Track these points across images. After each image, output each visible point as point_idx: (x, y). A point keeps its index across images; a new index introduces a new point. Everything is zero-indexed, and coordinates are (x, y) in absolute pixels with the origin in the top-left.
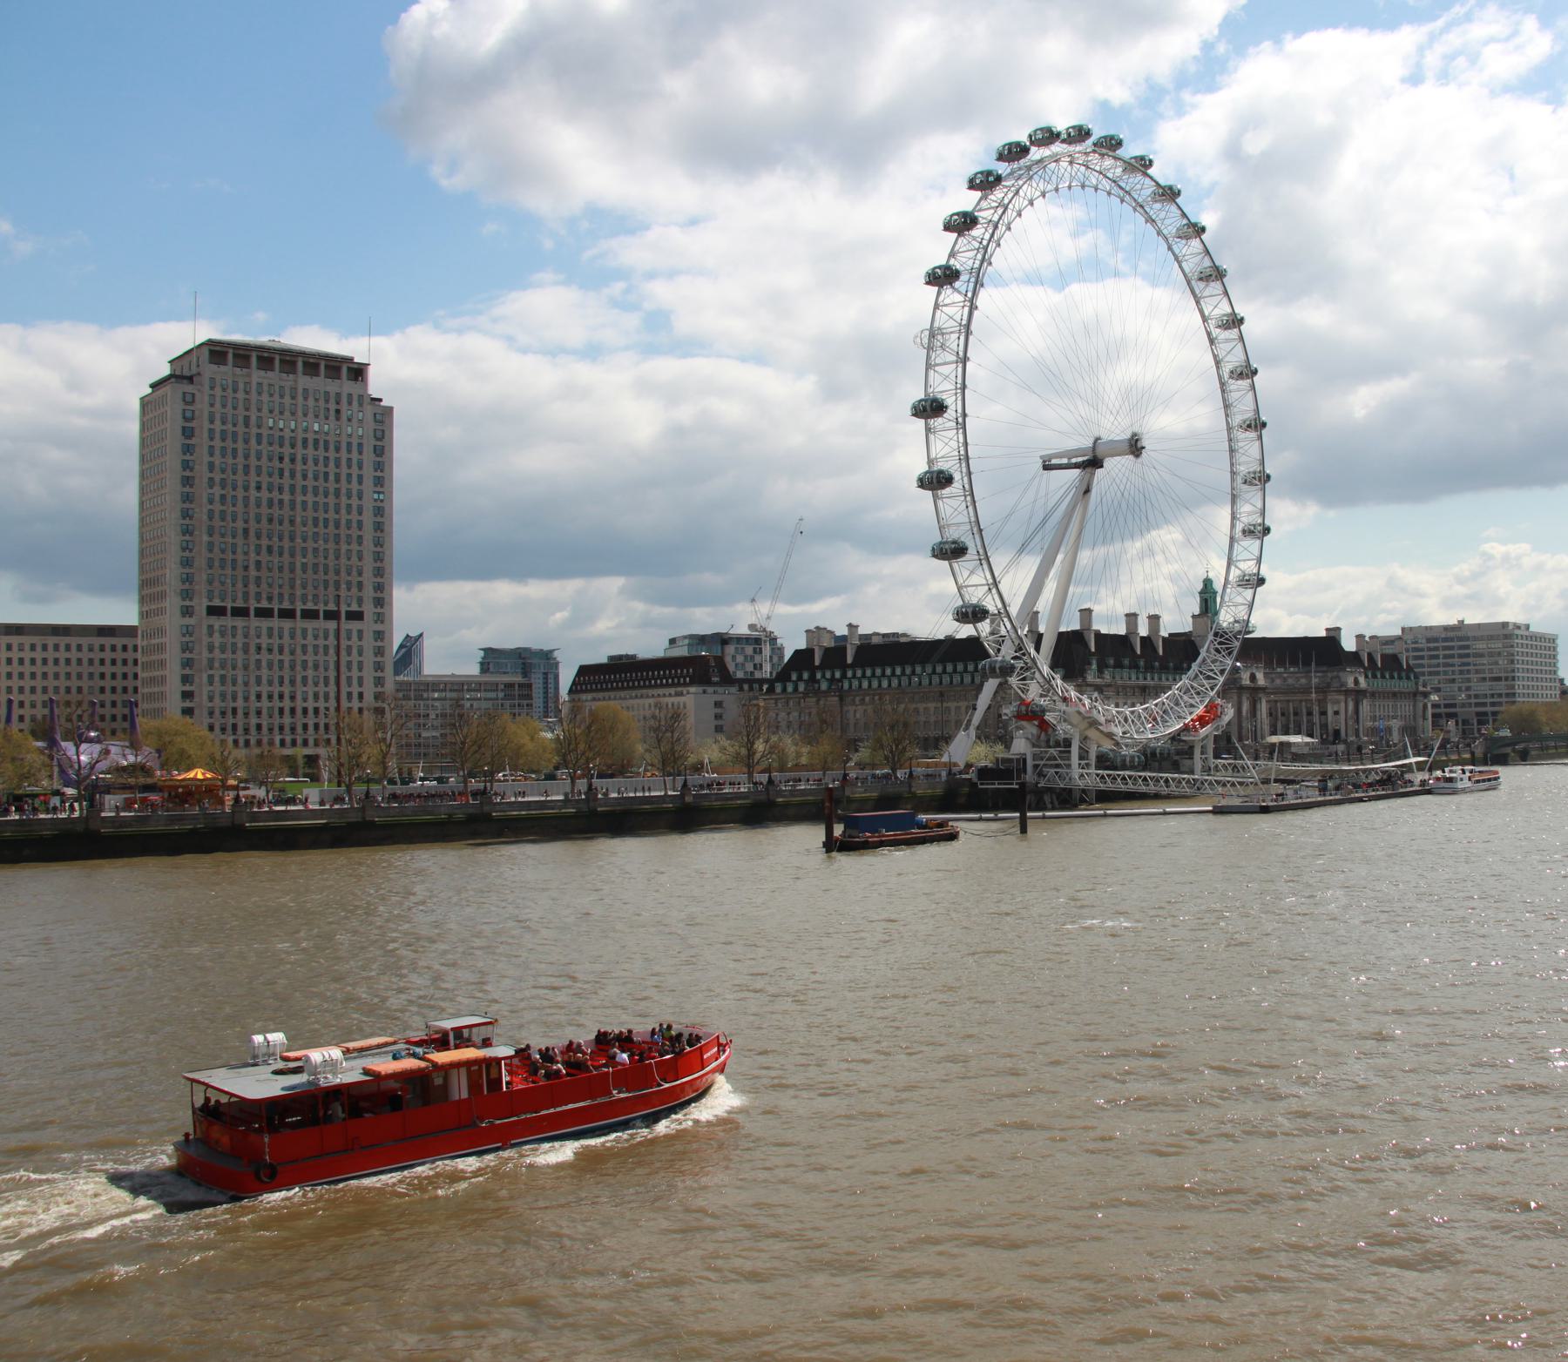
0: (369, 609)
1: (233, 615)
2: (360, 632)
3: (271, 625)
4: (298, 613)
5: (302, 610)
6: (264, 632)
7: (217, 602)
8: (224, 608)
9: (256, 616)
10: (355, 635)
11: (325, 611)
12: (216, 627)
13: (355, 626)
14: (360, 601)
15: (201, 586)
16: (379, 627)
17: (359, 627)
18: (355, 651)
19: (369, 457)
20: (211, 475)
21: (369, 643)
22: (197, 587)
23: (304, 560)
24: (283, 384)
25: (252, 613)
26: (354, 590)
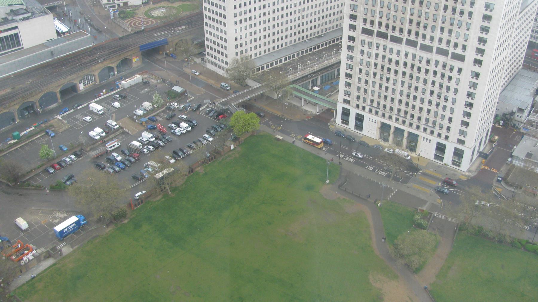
0: (470, 55)
1: (377, 36)
2: (460, 70)
3: (399, 49)
6: (395, 52)
7: (368, 26)
10: (456, 70)
11: (438, 49)
12: (366, 42)
13: (457, 64)
16: (477, 69)
17: (461, 67)
21: (466, 78)
22: (359, 14)
23: (428, 11)
25: (389, 38)
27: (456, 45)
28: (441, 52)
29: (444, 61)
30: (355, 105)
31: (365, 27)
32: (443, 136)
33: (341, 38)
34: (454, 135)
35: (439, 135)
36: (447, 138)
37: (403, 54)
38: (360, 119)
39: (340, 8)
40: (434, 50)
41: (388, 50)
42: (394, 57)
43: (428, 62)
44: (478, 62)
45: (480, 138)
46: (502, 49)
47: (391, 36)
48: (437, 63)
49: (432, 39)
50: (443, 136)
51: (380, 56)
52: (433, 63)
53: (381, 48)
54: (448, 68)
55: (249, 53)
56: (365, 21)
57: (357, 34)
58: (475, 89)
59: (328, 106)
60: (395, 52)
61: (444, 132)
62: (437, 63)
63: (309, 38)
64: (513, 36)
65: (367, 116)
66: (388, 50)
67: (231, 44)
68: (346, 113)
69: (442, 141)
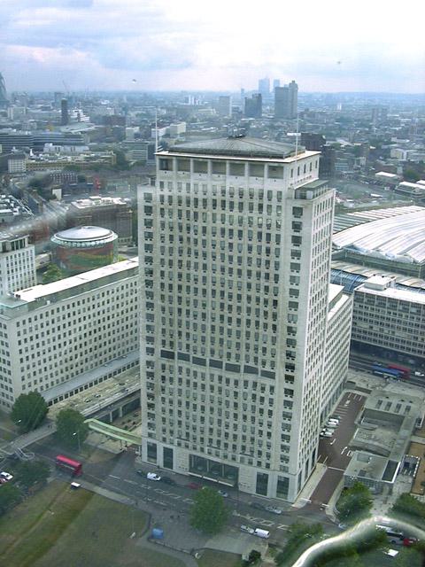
2: (272, 388)
4: (224, 365)
5: (226, 364)
7: (167, 348)
8: (173, 353)
9: (193, 363)
13: (268, 382)
14: (273, 364)
15: (159, 337)
16: (289, 386)
18: (266, 401)
19: (287, 246)
20: (162, 257)
21: (279, 397)
24: (214, 183)
26: (268, 355)
27: (264, 363)
28: (249, 370)
29: (255, 380)
30: (161, 439)
31: (163, 349)
32: (264, 464)
33: (137, 362)
34: (275, 463)
35: (259, 464)
36: (268, 466)
37: (208, 377)
38: (168, 453)
39: (135, 335)
40: (242, 369)
41: (192, 373)
42: (199, 381)
43: (236, 383)
44: (289, 379)
45: (305, 461)
46: (314, 360)
47: (193, 357)
48: (246, 383)
49: (238, 357)
50: (264, 464)
51: (184, 380)
52: (241, 384)
53: (184, 371)
54: (259, 388)
55: (38, 386)
56: (164, 342)
57: (155, 358)
58: (290, 409)
59: (130, 442)
60: (199, 375)
61: (264, 459)
62: (246, 383)
63: (108, 361)
64: (326, 346)
65: (177, 451)
66: (192, 373)
67: (16, 376)
68: (152, 449)
69: (263, 471)
